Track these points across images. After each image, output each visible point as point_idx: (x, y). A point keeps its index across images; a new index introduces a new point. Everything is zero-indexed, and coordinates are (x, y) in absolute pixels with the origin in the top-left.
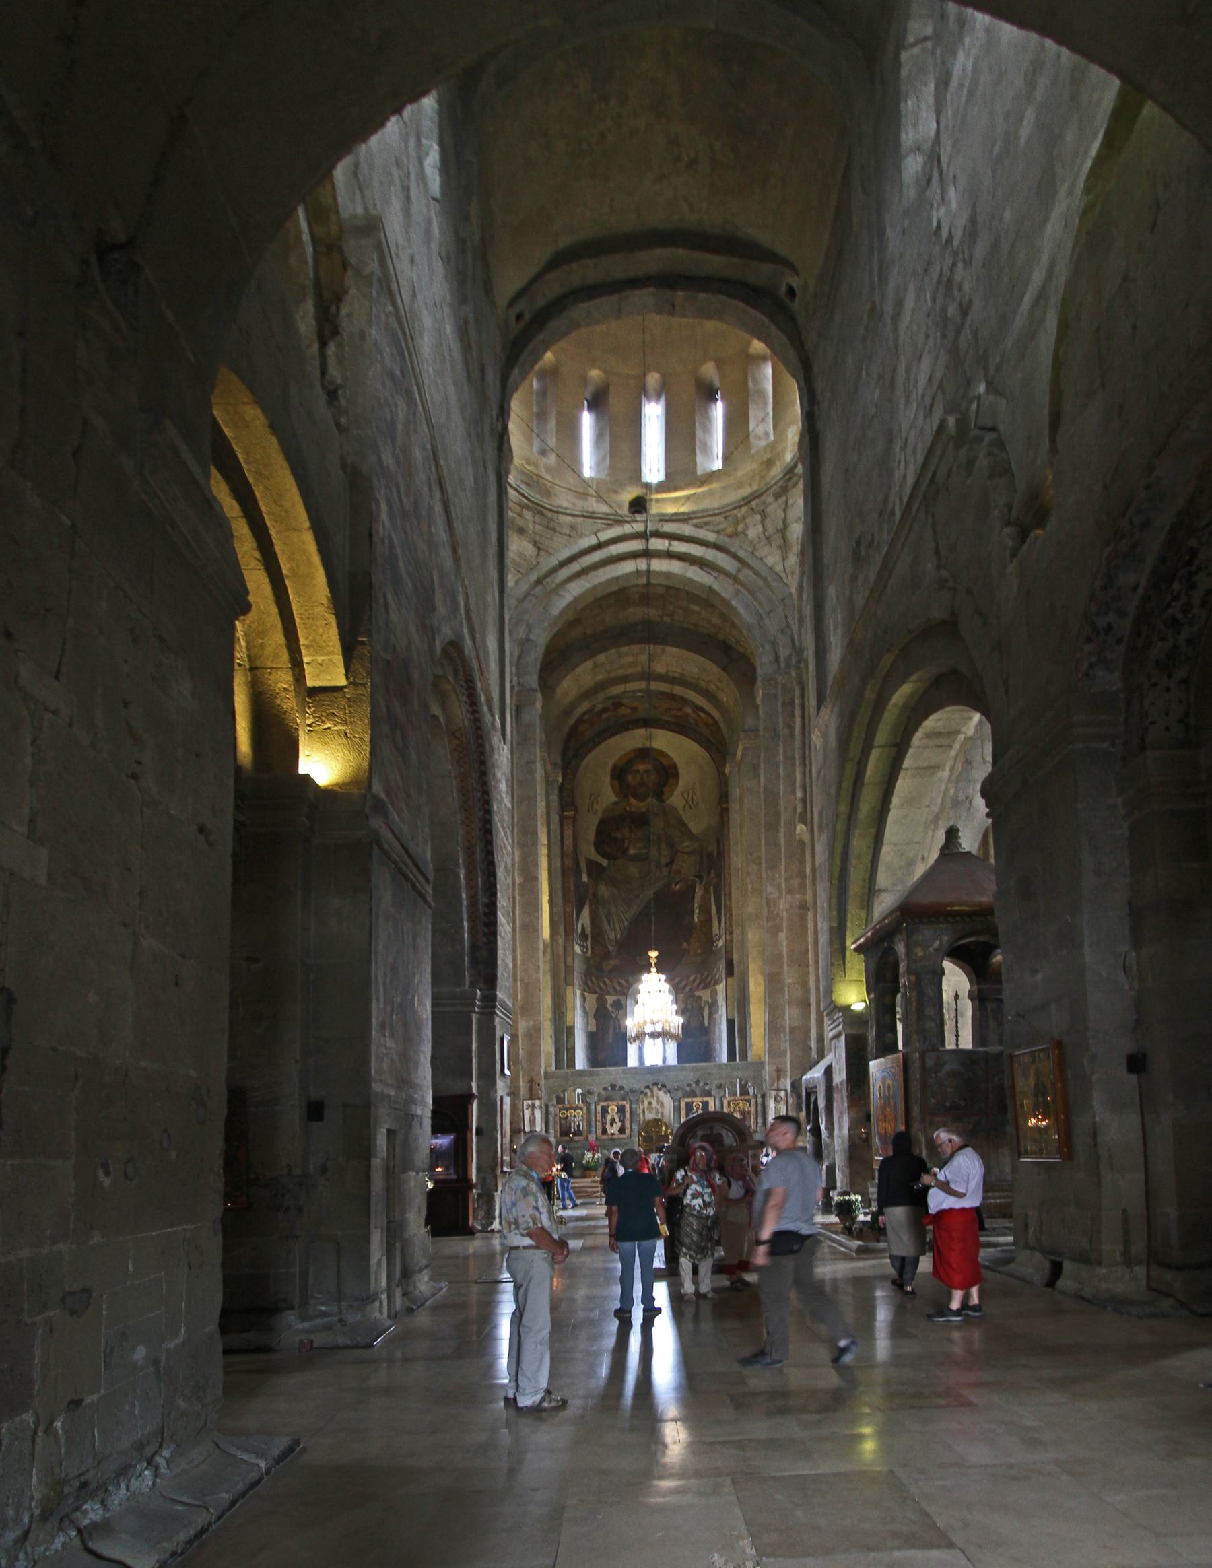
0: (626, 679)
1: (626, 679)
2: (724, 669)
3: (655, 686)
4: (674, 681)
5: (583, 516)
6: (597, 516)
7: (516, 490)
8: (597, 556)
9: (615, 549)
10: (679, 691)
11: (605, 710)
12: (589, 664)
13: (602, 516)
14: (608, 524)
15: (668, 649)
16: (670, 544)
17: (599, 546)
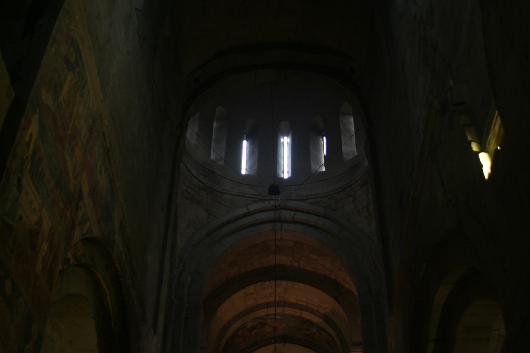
0: (268, 305)
1: (268, 305)
2: (336, 299)
3: (289, 311)
4: (302, 308)
5: (239, 196)
6: (248, 195)
7: (197, 178)
8: (247, 221)
9: (259, 217)
10: (305, 315)
11: (253, 328)
12: (241, 293)
13: (251, 196)
14: (255, 201)
15: (296, 284)
16: (294, 214)
17: (248, 214)
